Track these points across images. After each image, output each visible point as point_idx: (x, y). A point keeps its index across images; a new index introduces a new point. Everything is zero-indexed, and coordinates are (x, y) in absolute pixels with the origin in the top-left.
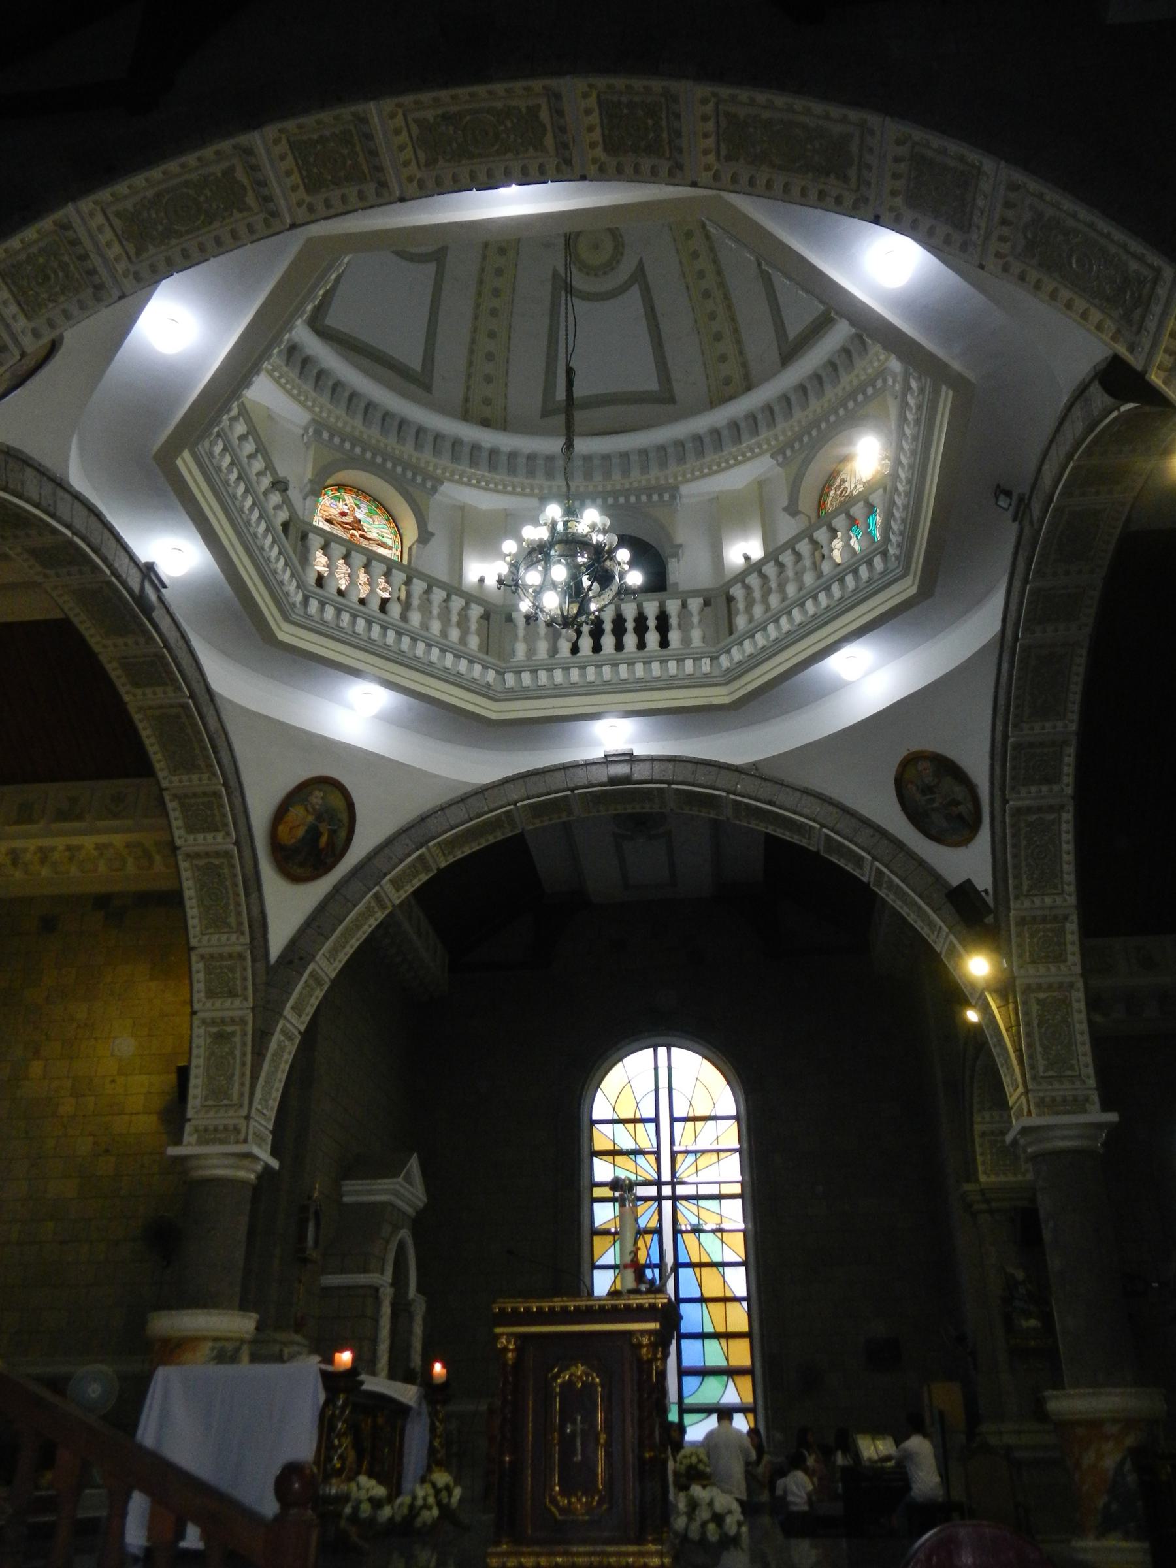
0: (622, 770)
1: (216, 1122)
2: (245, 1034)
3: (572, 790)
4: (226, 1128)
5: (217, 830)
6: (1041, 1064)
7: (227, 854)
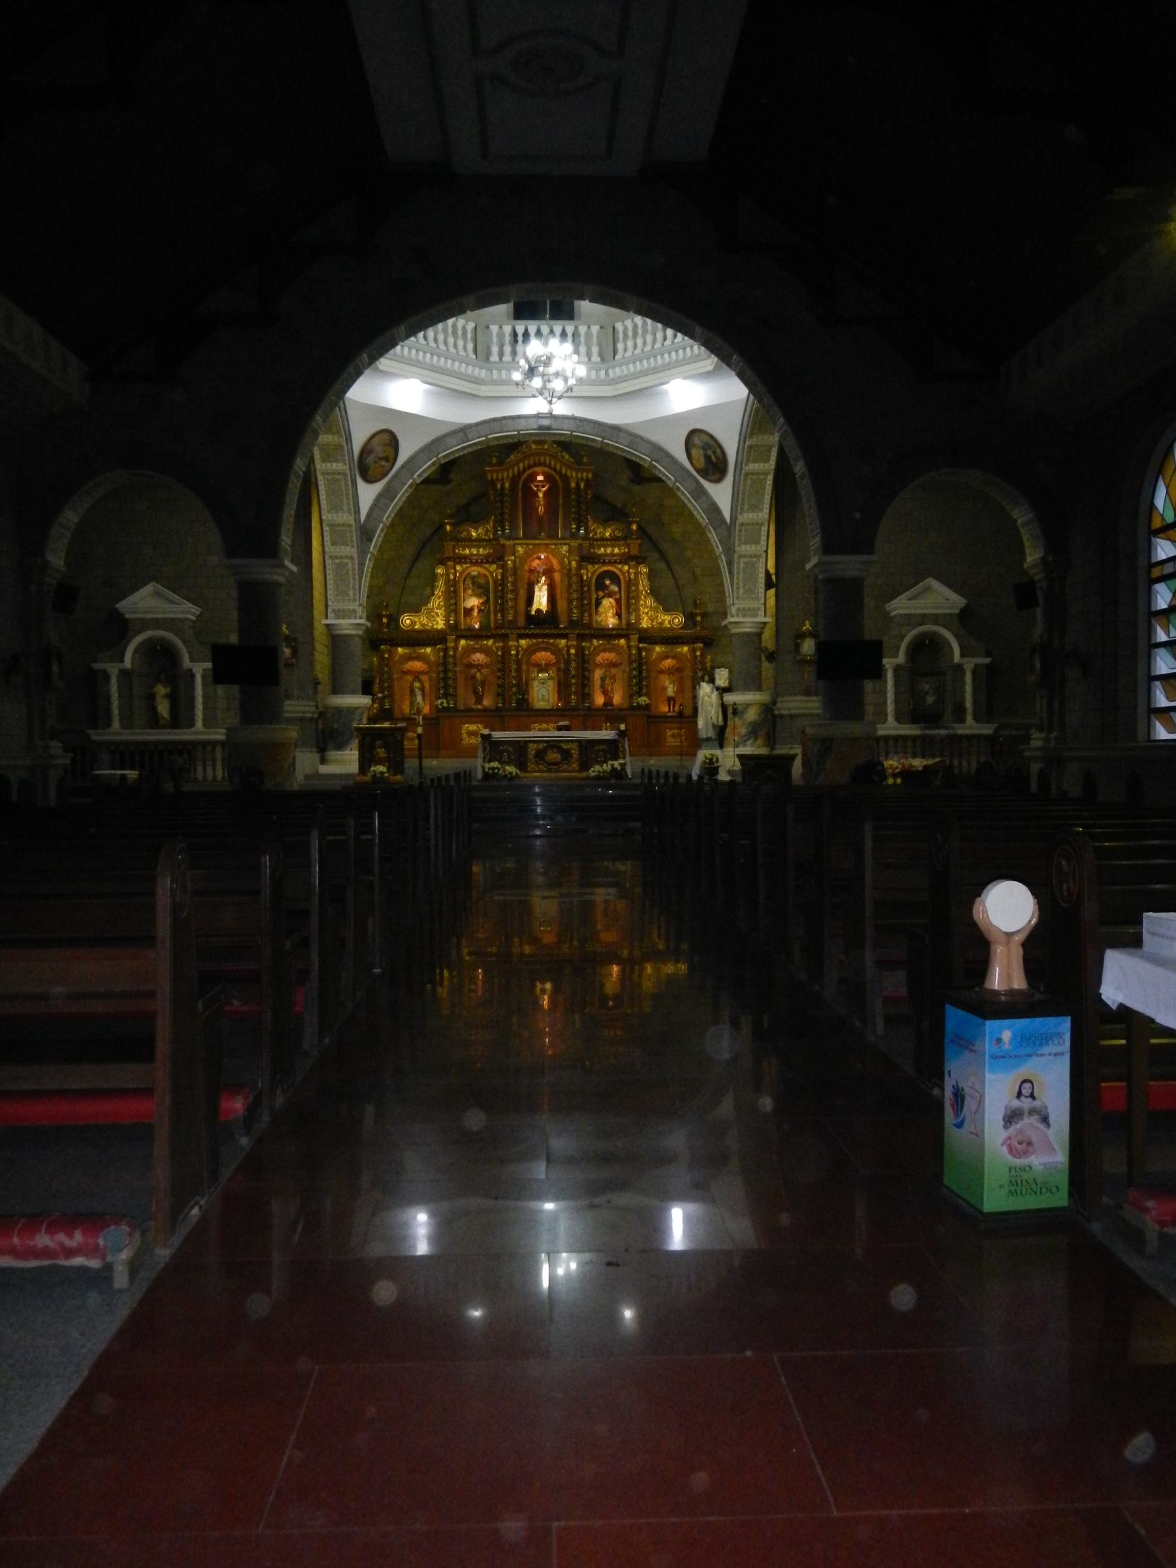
0: (546, 422)
1: (344, 607)
2: (354, 564)
3: (519, 431)
4: (349, 610)
5: (336, 461)
6: (741, 591)
7: (345, 474)
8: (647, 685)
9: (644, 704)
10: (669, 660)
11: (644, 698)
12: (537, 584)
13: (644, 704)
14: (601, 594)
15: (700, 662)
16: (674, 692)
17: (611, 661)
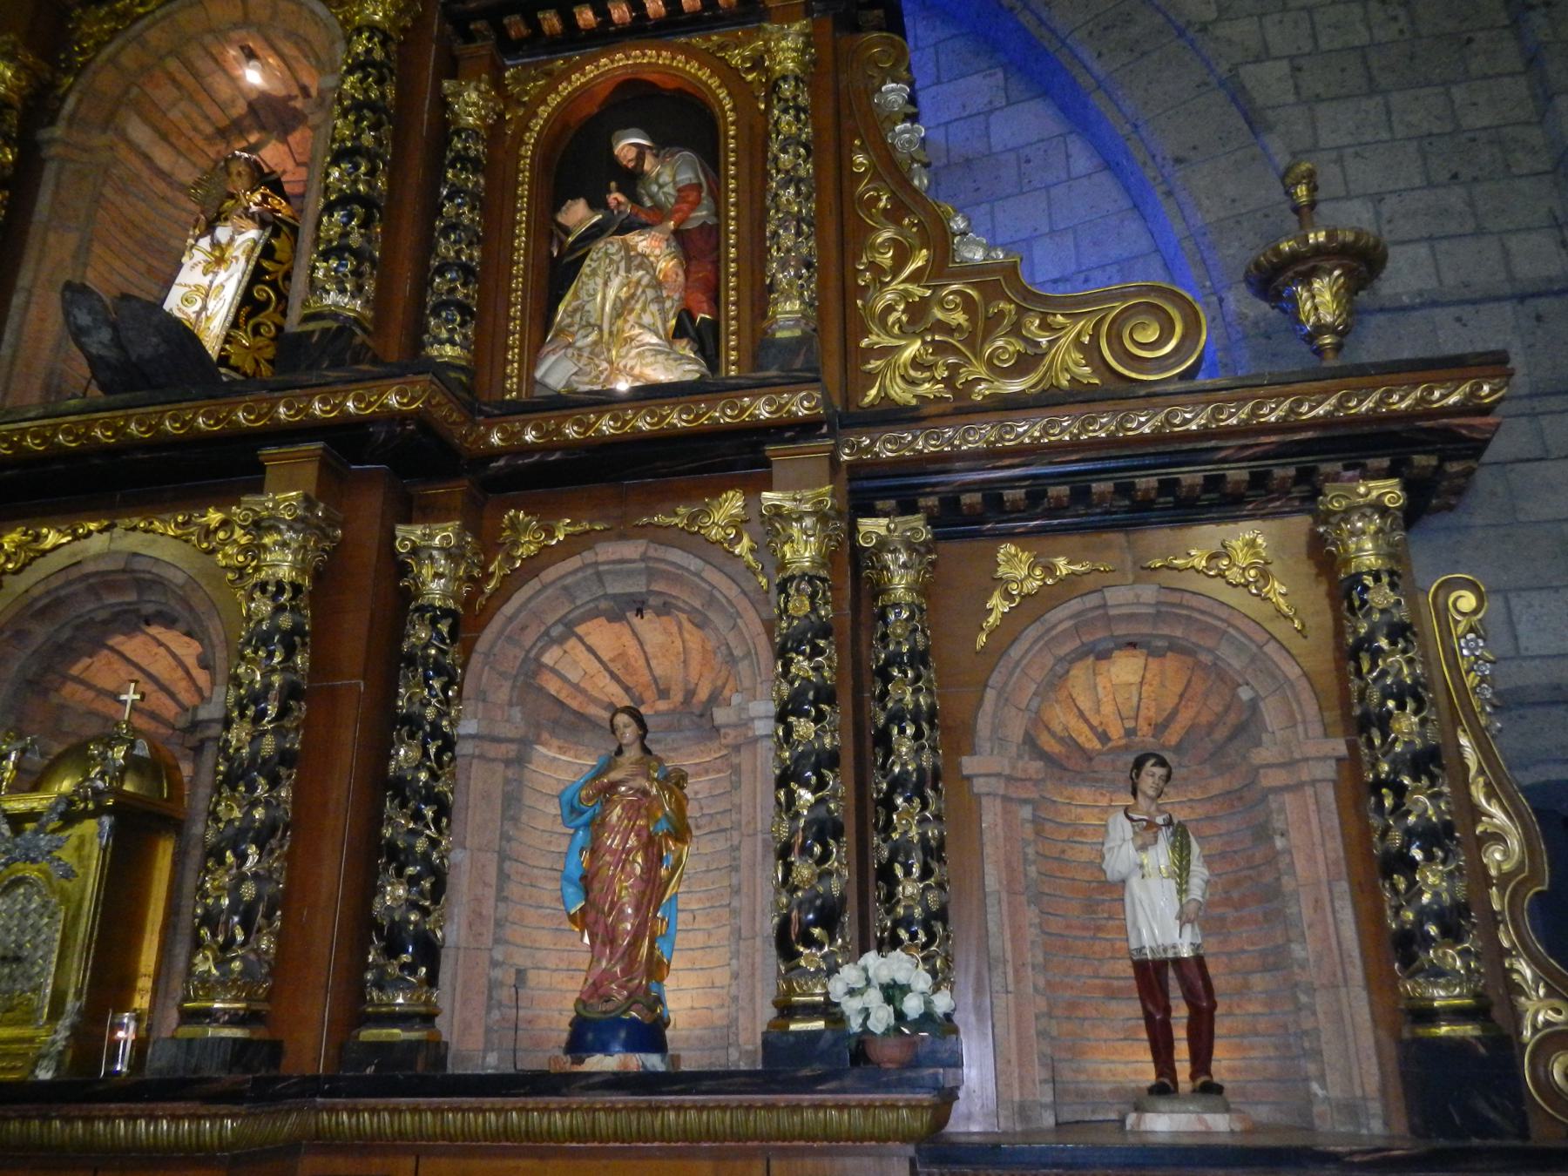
8: (933, 852)
9: (881, 1018)
10: (1125, 669)
11: (899, 966)
12: (210, 228)
13: (881, 1018)
14: (577, 215)
15: (1398, 631)
16: (1183, 918)
17: (690, 694)
